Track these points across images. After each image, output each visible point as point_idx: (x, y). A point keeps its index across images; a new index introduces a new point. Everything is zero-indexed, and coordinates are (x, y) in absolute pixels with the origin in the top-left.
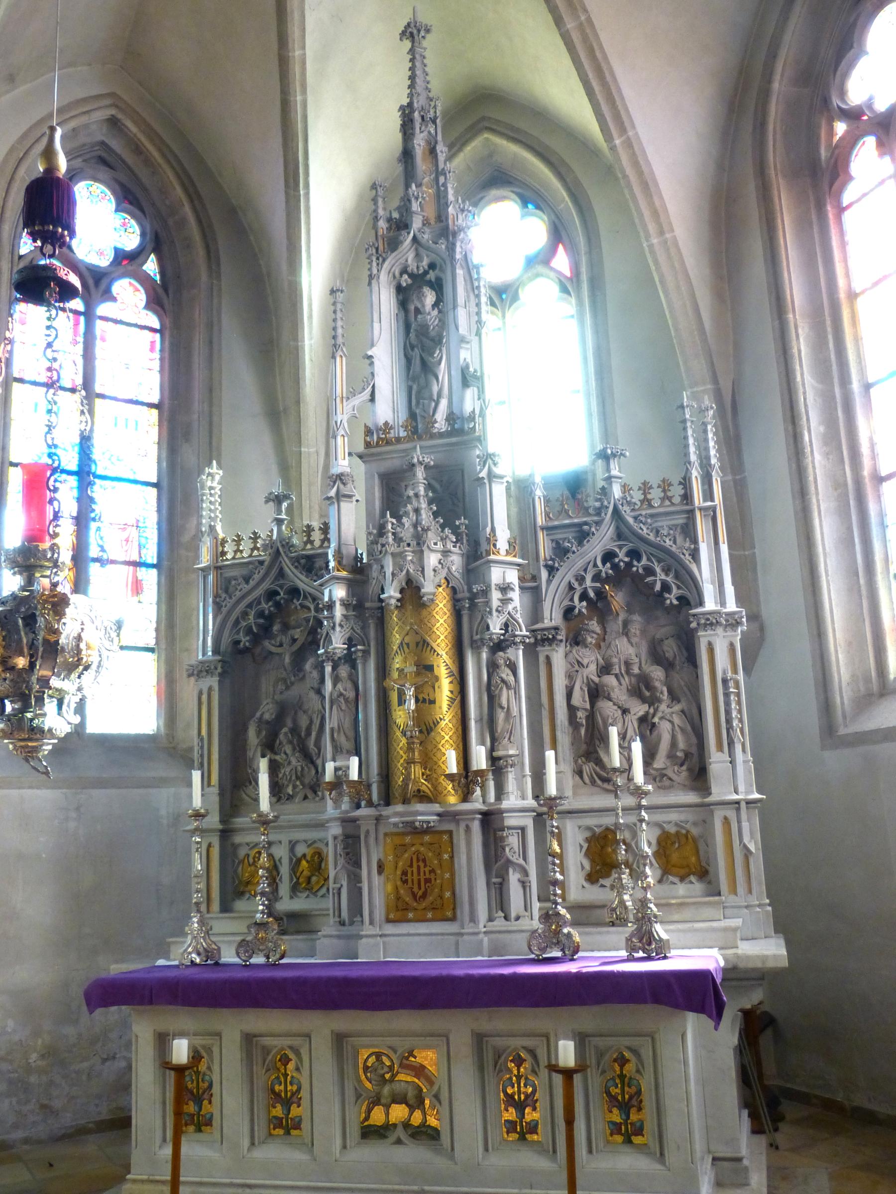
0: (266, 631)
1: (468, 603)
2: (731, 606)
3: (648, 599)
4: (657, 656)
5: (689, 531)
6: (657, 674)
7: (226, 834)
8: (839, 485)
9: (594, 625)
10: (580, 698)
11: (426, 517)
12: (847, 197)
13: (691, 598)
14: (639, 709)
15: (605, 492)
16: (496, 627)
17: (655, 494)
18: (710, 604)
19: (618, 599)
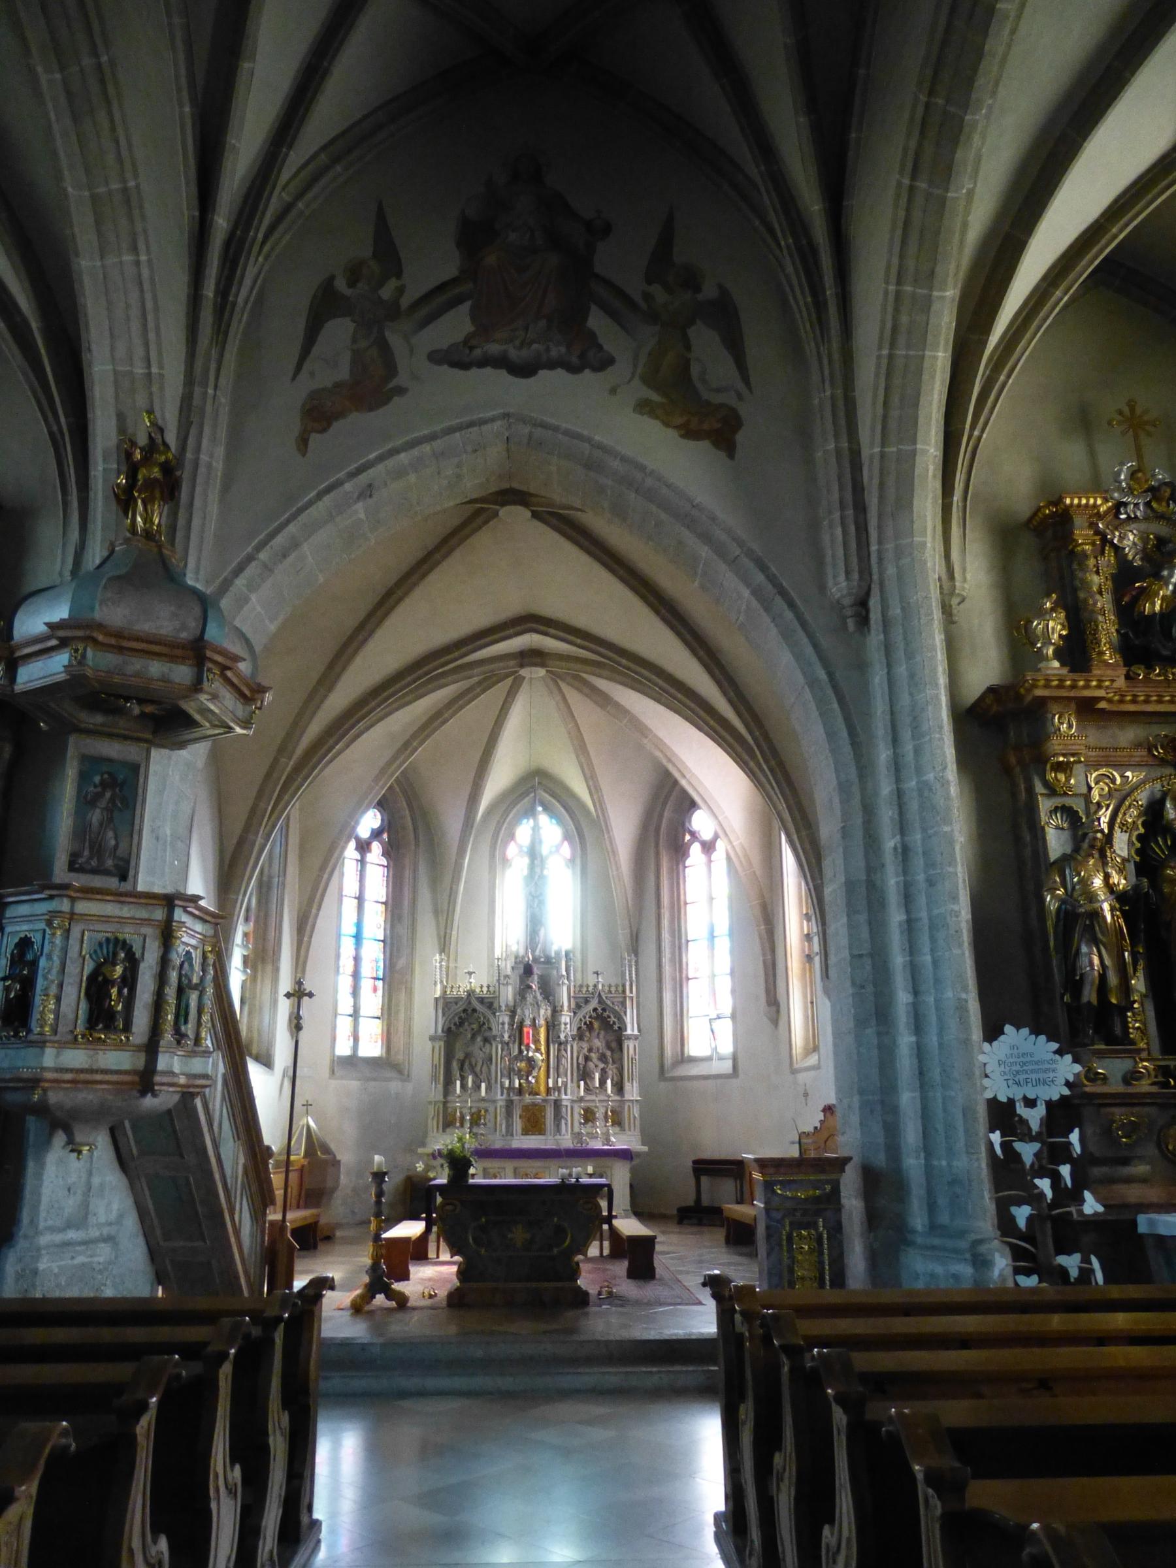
0: (461, 1024)
1: (552, 1026)
2: (636, 1032)
3: (606, 1025)
4: (609, 1047)
5: (623, 1004)
6: (609, 1053)
7: (445, 1103)
8: (674, 979)
9: (587, 1034)
10: (581, 1060)
11: (540, 998)
12: (688, 863)
13: (622, 1028)
14: (602, 1066)
15: (595, 986)
16: (562, 1036)
17: (613, 989)
18: (629, 1032)
19: (596, 1025)
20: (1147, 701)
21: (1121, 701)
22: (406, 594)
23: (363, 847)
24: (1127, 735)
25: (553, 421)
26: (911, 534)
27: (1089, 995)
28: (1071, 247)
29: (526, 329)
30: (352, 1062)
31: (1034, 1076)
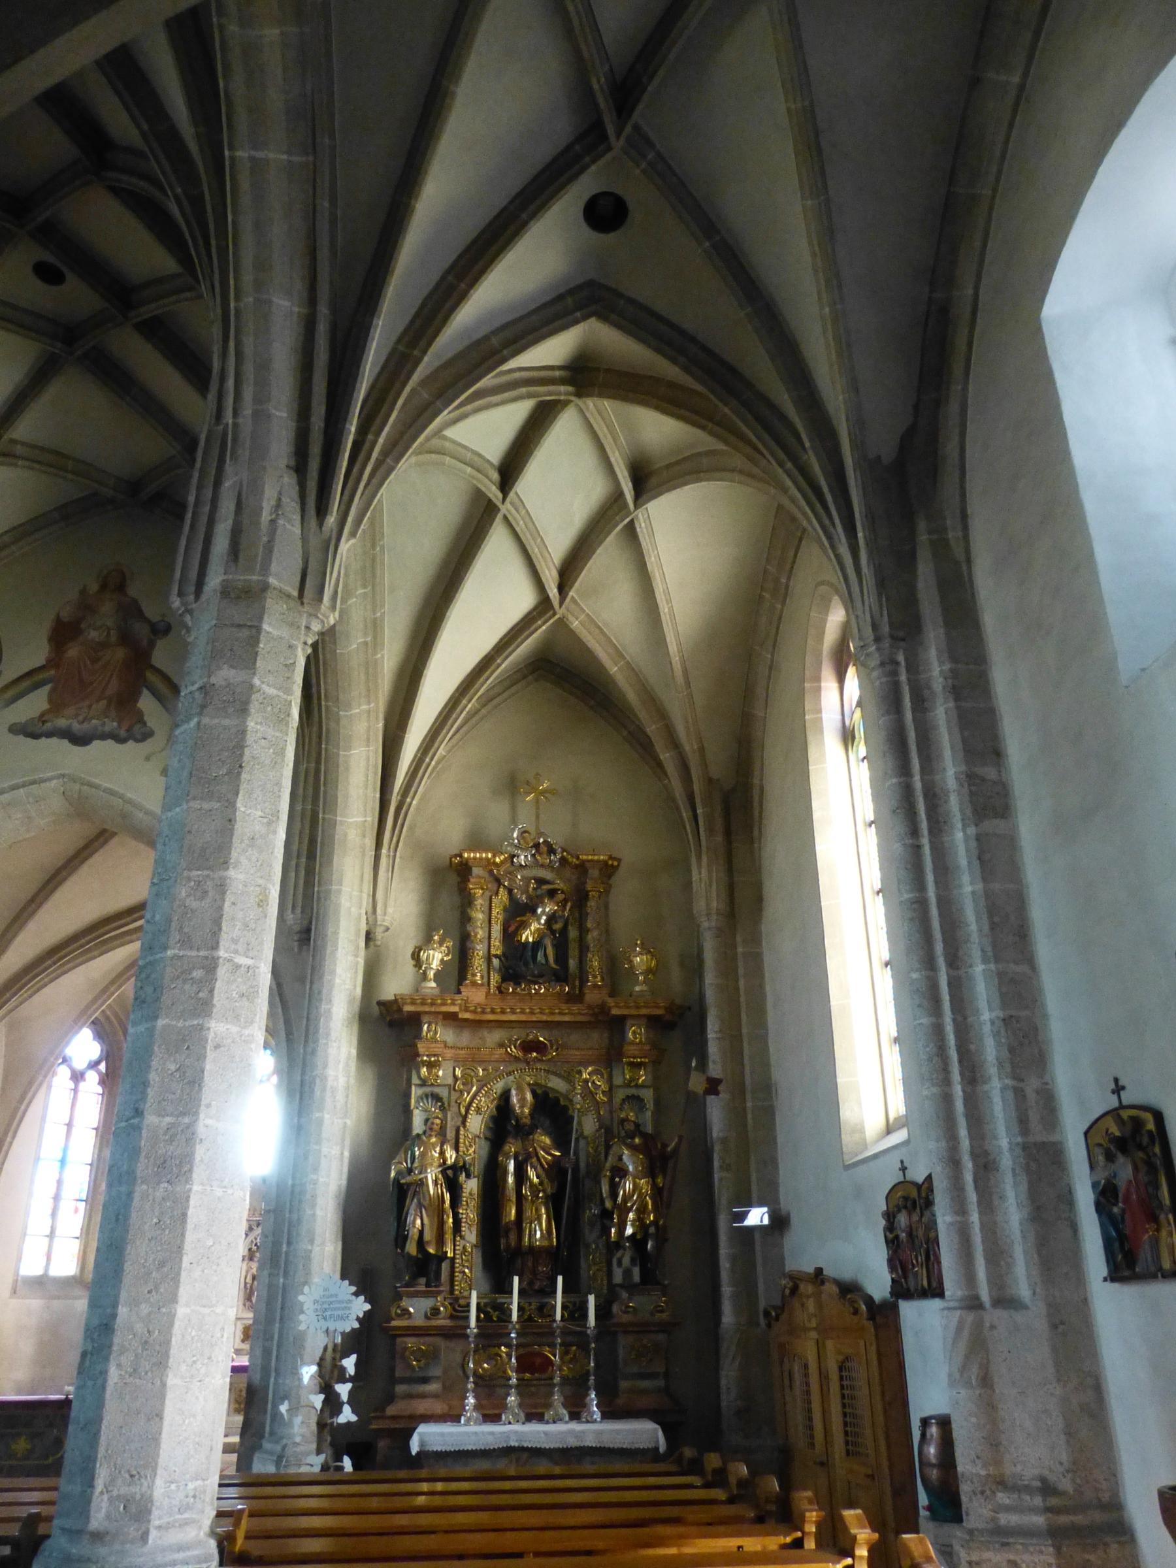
20: (503, 1012)
21: (483, 1012)
22: (70, 874)
23: (77, 1077)
24: (493, 1037)
25: (97, 781)
26: (330, 882)
27: (411, 1248)
28: (474, 669)
29: (90, 706)
30: (41, 1283)
31: (336, 1313)
